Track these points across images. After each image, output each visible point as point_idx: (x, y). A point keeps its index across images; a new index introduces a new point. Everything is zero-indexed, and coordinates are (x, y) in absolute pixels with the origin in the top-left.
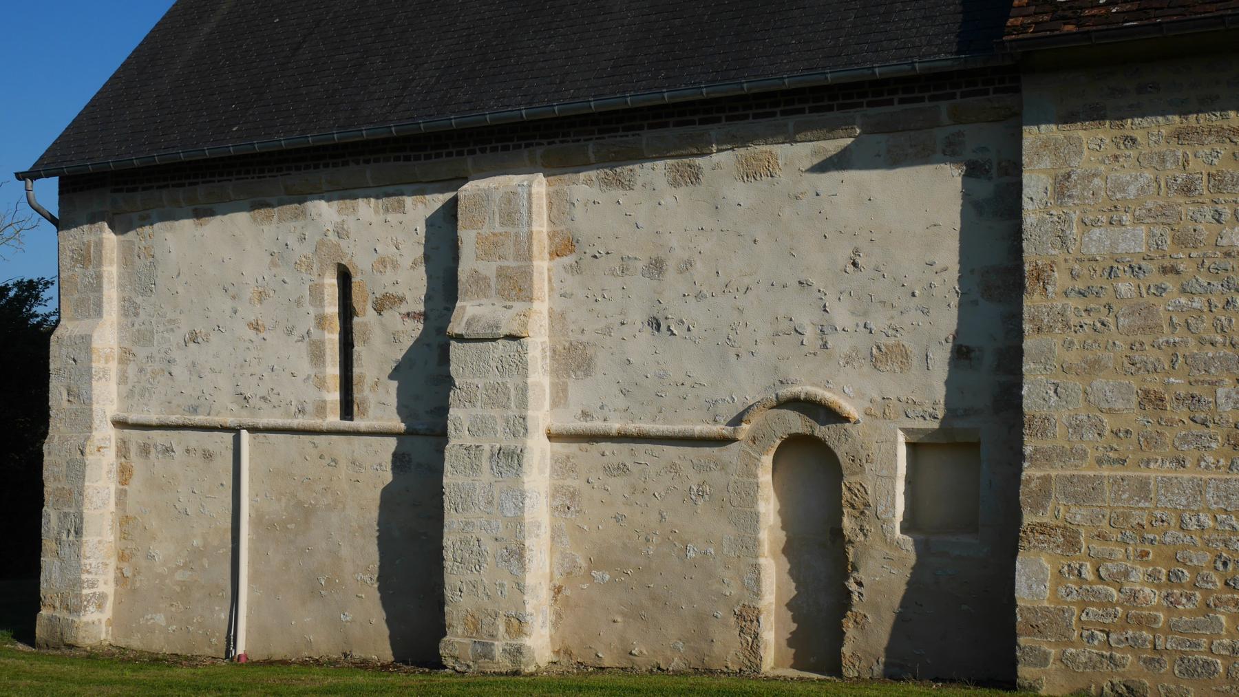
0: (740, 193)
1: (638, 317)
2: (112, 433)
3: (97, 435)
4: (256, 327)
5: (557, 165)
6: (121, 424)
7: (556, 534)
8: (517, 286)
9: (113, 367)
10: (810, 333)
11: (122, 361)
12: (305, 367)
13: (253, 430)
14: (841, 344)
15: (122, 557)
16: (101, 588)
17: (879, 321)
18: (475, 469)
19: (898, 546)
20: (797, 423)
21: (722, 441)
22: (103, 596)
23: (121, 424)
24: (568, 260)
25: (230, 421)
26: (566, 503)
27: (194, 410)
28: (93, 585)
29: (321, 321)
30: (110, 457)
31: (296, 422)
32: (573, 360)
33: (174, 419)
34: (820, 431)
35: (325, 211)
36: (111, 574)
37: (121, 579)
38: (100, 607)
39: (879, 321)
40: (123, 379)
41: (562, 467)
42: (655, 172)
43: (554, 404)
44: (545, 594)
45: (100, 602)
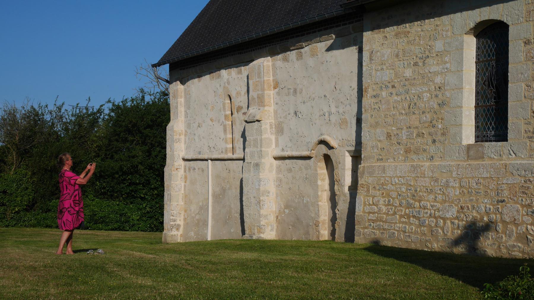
0: (311, 62)
1: (292, 112)
2: (183, 163)
3: (176, 164)
4: (212, 120)
5: (273, 53)
6: (184, 160)
7: (277, 196)
8: (261, 101)
9: (183, 137)
10: (327, 114)
11: (185, 135)
12: (222, 135)
13: (212, 160)
14: (333, 118)
15: (185, 211)
16: (178, 222)
17: (341, 111)
18: (249, 171)
19: (345, 195)
20: (323, 149)
21: (309, 158)
22: (179, 226)
23: (184, 160)
24: (277, 90)
25: (206, 157)
26: (279, 182)
27: (200, 153)
28: (175, 221)
29: (226, 116)
30: (181, 172)
31: (220, 157)
32: (279, 130)
33: (194, 157)
34: (329, 152)
35: (224, 72)
36: (182, 218)
37: (185, 219)
38: (178, 229)
39: (341, 111)
40: (185, 142)
41: (279, 170)
42: (292, 55)
43: (276, 146)
44: (272, 218)
45: (178, 227)
